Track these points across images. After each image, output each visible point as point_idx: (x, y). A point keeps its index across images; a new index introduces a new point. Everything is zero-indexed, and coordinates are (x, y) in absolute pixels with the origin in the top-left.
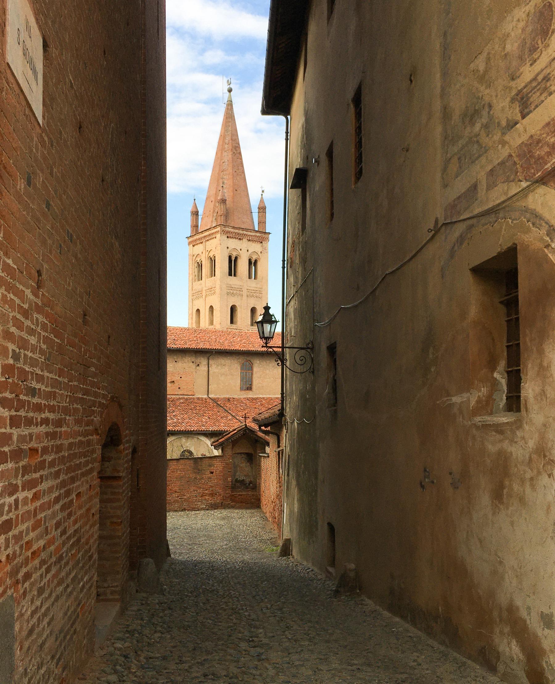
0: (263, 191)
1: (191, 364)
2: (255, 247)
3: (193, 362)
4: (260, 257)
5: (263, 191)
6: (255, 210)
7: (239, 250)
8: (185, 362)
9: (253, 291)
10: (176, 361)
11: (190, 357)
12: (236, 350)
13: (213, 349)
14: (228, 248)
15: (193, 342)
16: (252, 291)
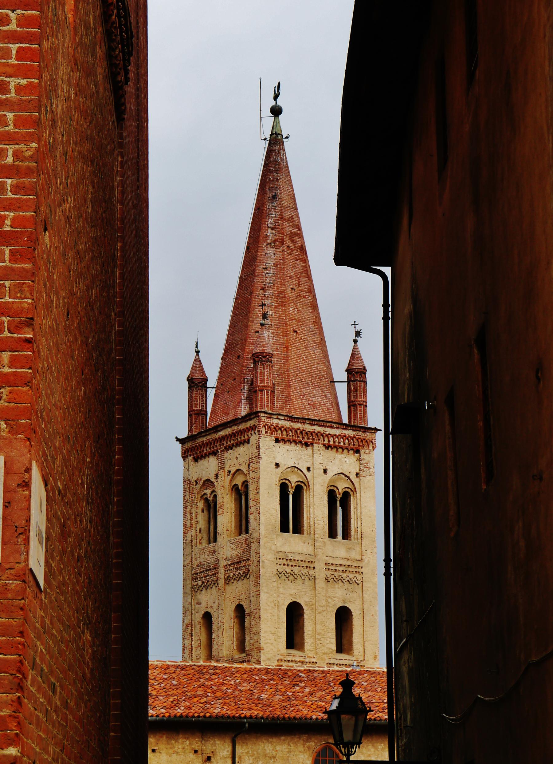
0: (358, 334)
1: (192, 756)
3: (196, 752)
4: (357, 485)
5: (358, 334)
7: (305, 471)
8: (174, 752)
9: (341, 568)
11: (188, 738)
12: (300, 718)
13: (245, 717)
14: (277, 465)
15: (195, 700)
16: (337, 568)
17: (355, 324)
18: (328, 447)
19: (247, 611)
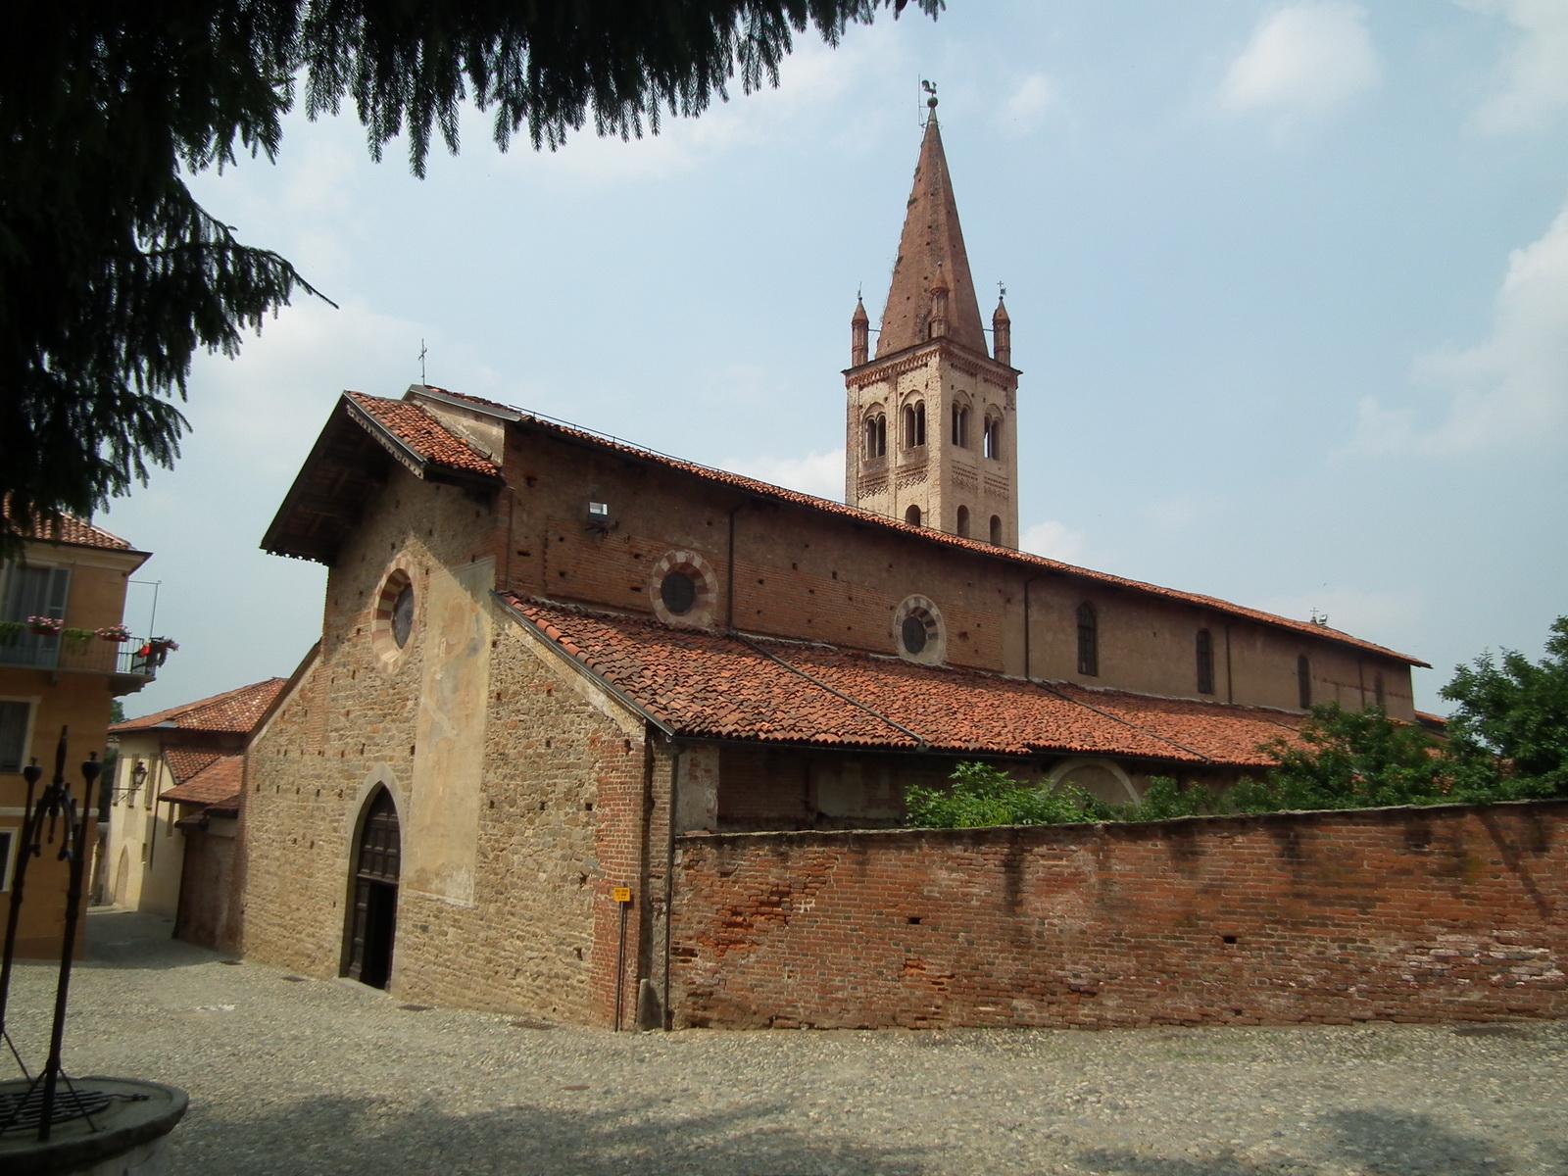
0: (1003, 291)
2: (997, 397)
5: (1003, 291)
6: (987, 322)
10: (969, 584)
17: (1000, 284)
18: (986, 380)
19: (923, 509)
